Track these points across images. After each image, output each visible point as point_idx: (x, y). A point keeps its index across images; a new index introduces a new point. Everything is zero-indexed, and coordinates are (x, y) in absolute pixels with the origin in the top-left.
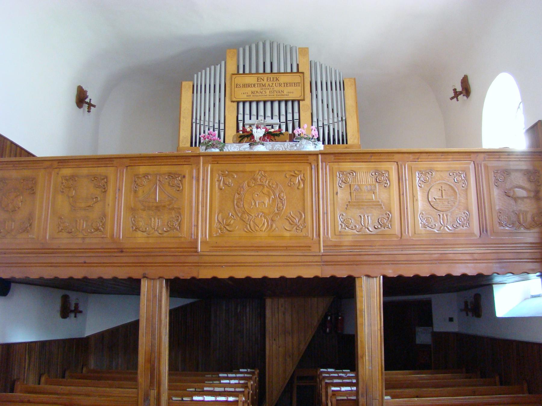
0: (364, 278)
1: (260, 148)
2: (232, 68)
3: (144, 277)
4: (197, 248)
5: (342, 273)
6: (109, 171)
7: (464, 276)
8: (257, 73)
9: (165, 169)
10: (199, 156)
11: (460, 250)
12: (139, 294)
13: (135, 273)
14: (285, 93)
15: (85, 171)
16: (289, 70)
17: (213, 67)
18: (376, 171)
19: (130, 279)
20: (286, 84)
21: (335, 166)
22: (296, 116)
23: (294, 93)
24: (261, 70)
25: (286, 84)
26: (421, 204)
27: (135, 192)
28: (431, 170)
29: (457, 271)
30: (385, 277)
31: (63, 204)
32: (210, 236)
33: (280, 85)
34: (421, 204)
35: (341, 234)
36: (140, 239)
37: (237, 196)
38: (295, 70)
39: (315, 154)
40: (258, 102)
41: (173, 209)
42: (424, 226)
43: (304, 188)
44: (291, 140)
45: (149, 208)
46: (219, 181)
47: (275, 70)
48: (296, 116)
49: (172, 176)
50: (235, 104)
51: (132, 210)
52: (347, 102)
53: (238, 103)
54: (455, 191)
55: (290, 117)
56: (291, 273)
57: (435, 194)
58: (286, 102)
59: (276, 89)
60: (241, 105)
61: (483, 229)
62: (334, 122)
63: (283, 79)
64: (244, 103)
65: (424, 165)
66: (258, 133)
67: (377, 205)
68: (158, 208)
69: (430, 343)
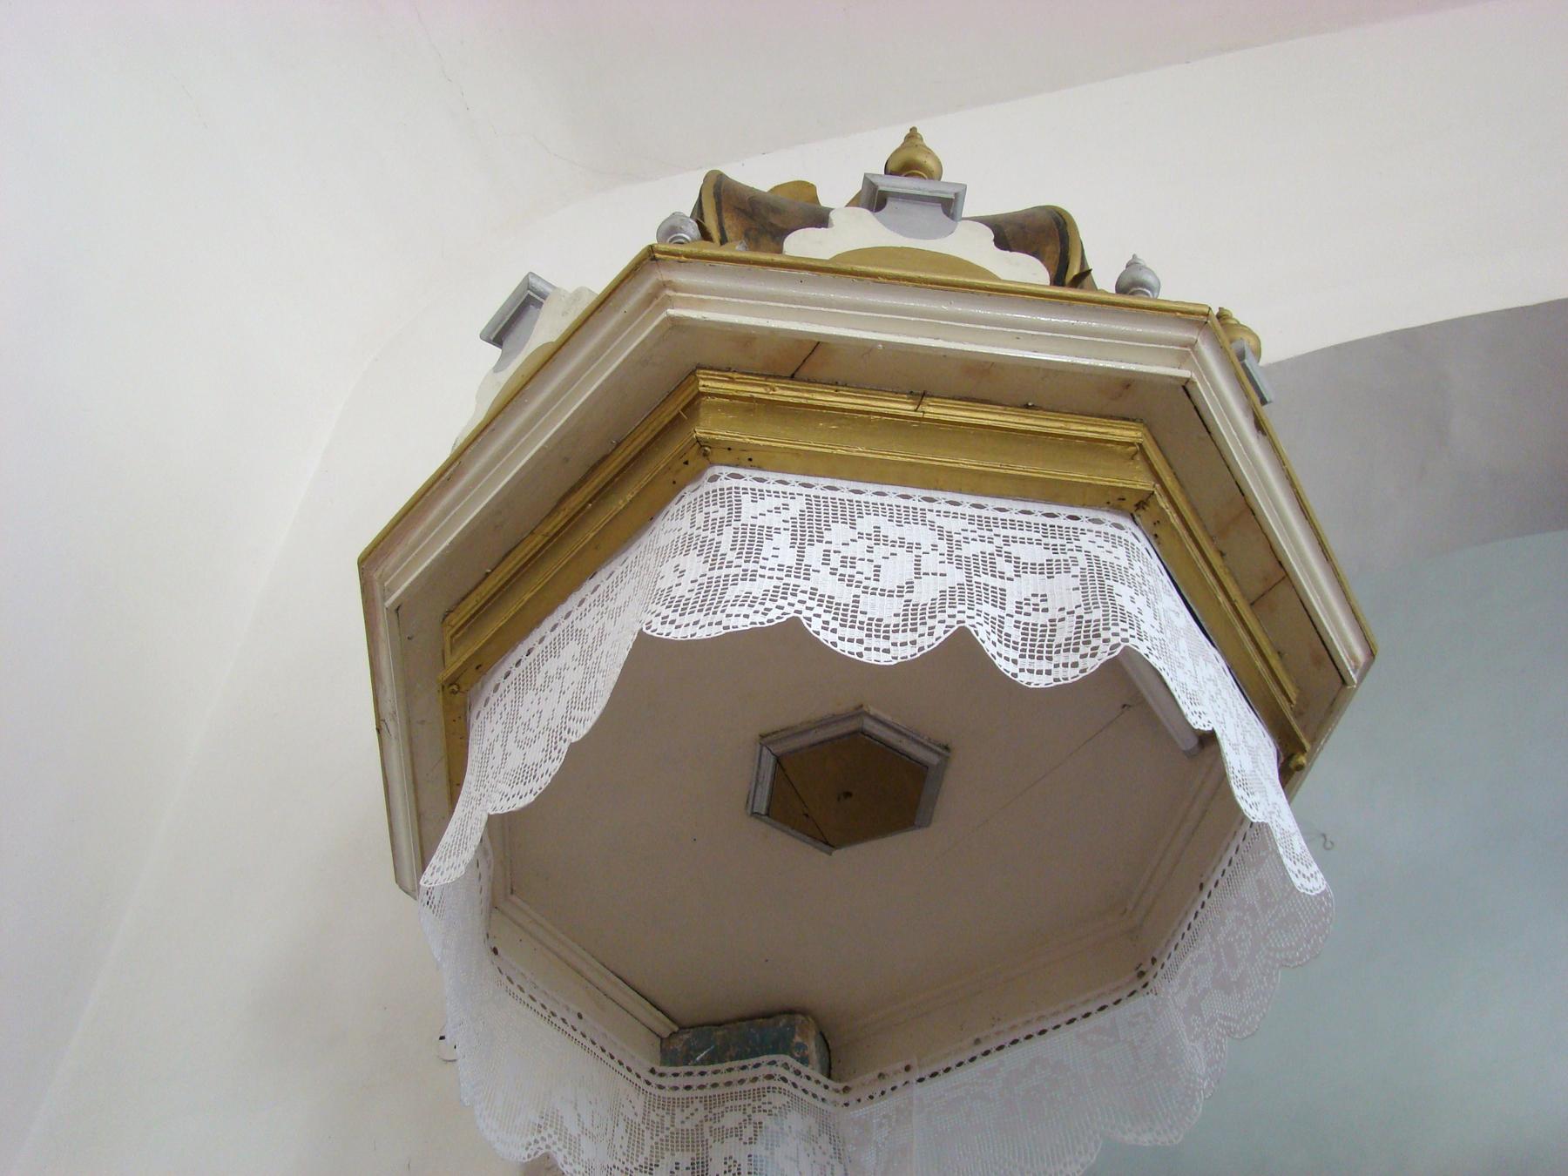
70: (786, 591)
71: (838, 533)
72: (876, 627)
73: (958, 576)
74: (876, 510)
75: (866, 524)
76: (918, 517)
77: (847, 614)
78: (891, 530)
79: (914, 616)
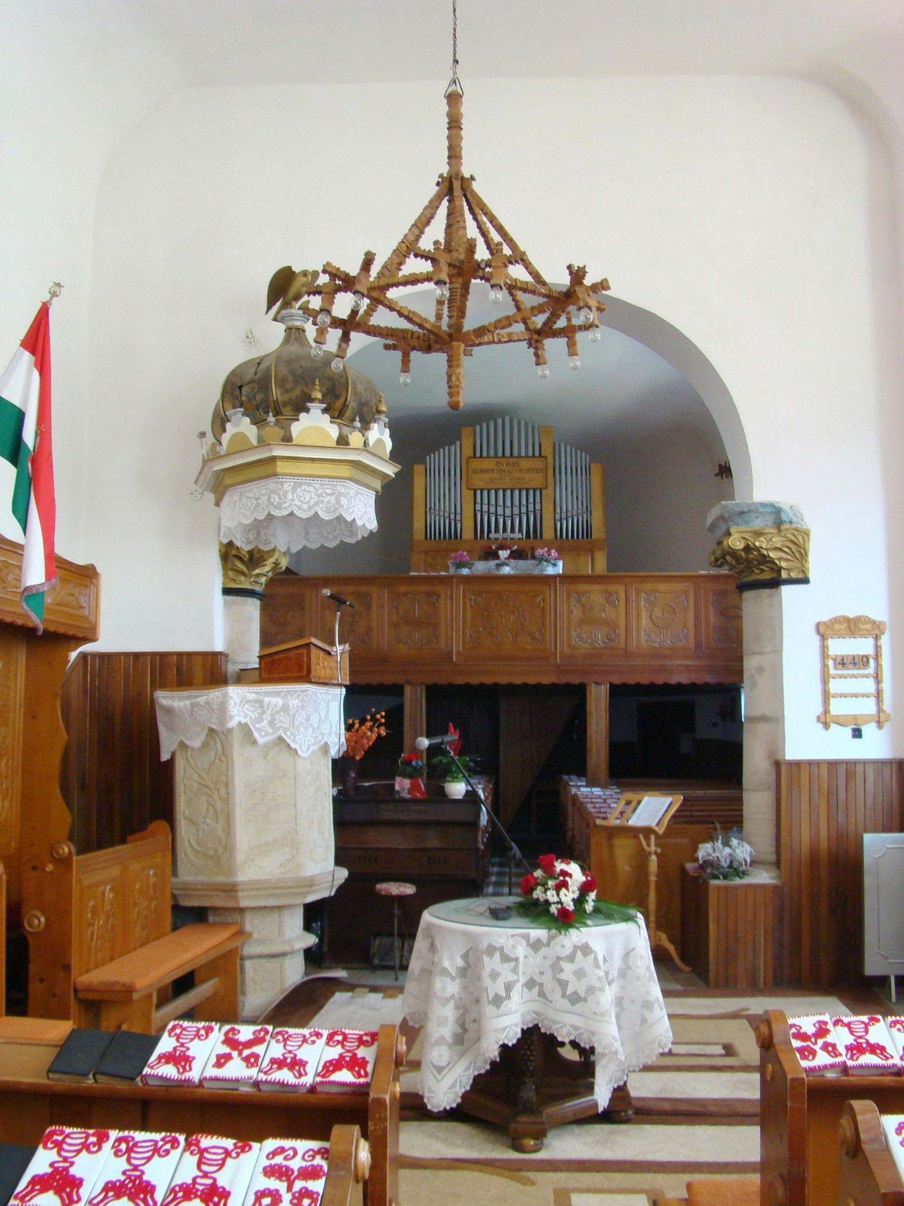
0: (593, 685)
1: (506, 570)
2: (468, 451)
3: (409, 683)
4: (451, 658)
5: (575, 680)
6: (374, 590)
7: (679, 685)
8: (496, 456)
9: (423, 588)
10: (452, 577)
11: (677, 662)
12: (403, 695)
13: (398, 679)
14: (527, 480)
16: (530, 454)
17: (447, 448)
18: (606, 592)
19: (395, 685)
20: (528, 471)
21: (572, 587)
22: (538, 507)
23: (536, 480)
24: (500, 454)
25: (528, 471)
26: (645, 621)
27: (397, 608)
28: (656, 591)
29: (674, 679)
30: (611, 685)
32: (463, 645)
33: (521, 471)
34: (645, 621)
35: (574, 648)
36: (402, 649)
37: (486, 613)
38: (537, 454)
39: (554, 577)
41: (430, 624)
42: (647, 641)
43: (543, 607)
44: (533, 557)
46: (471, 600)
47: (515, 453)
48: (538, 507)
49: (429, 594)
50: (472, 492)
51: (394, 625)
52: (593, 491)
53: (475, 491)
54: (674, 609)
55: (531, 508)
56: (532, 680)
57: (658, 613)
58: (527, 490)
59: (517, 475)
60: (479, 492)
61: (698, 645)
62: (578, 513)
64: (482, 491)
65: (649, 586)
66: (504, 554)
68: (417, 624)
70: (291, 505)
71: (299, 490)
72: (304, 511)
73: (317, 499)
74: (304, 484)
75: (303, 487)
76: (311, 485)
77: (299, 508)
78: (307, 489)
79: (310, 508)
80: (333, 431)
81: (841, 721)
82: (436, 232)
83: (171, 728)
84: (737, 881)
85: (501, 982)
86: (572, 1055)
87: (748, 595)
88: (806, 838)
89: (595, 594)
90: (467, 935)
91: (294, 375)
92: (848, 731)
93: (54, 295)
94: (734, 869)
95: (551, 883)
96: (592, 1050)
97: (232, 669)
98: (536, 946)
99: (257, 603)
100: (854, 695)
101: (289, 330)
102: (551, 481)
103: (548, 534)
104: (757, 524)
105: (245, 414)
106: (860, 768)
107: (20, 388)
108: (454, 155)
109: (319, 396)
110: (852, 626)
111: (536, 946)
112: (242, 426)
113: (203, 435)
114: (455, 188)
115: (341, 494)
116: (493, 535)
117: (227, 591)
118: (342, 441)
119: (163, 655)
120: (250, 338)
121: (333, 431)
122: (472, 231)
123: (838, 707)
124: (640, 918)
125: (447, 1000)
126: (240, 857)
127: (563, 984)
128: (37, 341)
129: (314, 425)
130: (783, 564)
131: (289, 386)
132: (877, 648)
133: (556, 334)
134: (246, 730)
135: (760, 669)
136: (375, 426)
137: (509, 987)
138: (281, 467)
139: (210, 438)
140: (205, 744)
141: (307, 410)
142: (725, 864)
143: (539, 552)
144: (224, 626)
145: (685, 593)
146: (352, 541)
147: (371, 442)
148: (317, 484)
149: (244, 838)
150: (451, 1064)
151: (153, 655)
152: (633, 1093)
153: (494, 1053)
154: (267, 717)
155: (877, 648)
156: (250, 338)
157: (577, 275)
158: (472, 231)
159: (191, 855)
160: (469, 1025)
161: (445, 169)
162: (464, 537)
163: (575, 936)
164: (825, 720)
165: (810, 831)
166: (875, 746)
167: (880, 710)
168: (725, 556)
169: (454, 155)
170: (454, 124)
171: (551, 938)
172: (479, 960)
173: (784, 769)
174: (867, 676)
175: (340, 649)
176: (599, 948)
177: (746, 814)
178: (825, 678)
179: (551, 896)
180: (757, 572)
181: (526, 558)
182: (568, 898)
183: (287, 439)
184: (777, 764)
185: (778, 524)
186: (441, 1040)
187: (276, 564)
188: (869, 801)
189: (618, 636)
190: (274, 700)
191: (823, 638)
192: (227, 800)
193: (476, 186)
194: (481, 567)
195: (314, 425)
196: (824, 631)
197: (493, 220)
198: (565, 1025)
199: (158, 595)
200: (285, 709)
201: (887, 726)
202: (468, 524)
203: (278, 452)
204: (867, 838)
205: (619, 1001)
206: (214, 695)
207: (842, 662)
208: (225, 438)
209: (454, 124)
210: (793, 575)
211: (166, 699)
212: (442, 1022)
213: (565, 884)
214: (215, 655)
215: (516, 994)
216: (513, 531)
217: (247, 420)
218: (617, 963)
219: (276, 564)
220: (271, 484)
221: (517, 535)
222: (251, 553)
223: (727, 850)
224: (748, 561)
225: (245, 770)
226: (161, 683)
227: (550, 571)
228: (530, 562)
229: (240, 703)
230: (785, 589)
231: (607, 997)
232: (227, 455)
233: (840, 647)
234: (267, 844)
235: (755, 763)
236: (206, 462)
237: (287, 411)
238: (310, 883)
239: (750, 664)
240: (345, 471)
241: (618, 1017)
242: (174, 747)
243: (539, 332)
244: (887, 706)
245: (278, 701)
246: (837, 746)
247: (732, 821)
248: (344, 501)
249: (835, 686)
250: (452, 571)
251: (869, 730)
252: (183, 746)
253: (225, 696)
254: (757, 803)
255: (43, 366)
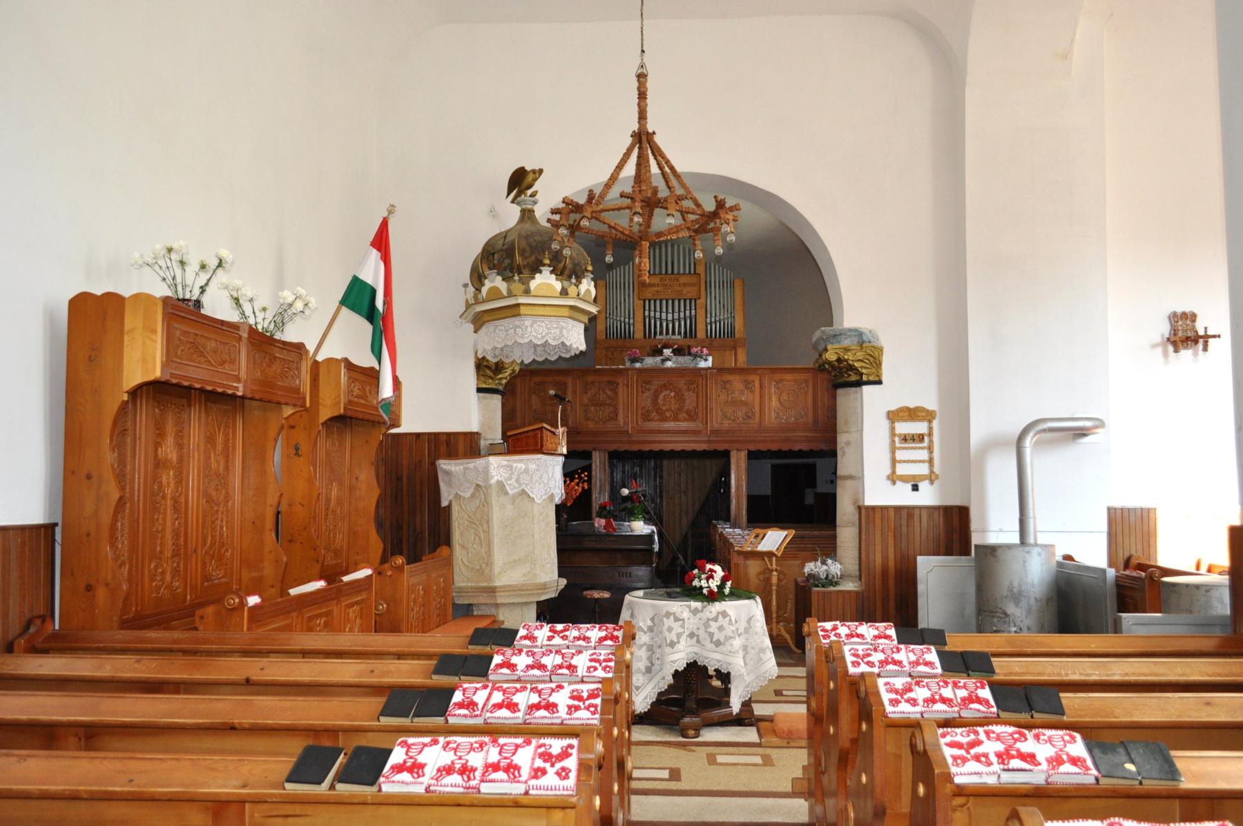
1: (669, 364)
5: (721, 447)
7: (801, 451)
9: (606, 379)
13: (587, 447)
15: (550, 379)
19: (585, 451)
20: (685, 285)
23: (690, 292)
25: (685, 285)
28: (782, 380)
29: (797, 447)
31: (535, 400)
34: (775, 403)
40: (661, 301)
44: (690, 354)
45: (596, 405)
49: (610, 383)
57: (785, 397)
61: (816, 420)
63: (683, 280)
65: (777, 376)
66: (667, 352)
67: (745, 404)
69: (769, 492)
80: (558, 286)
81: (904, 479)
82: (630, 170)
83: (449, 484)
84: (832, 588)
85: (674, 632)
86: (716, 683)
87: (840, 392)
88: (879, 560)
89: (737, 382)
90: (653, 606)
91: (531, 246)
92: (909, 486)
93: (390, 212)
94: (830, 581)
95: (703, 576)
96: (729, 674)
97: (483, 444)
98: (695, 612)
99: (500, 397)
100: (914, 461)
101: (523, 211)
102: (703, 293)
103: (701, 334)
104: (846, 343)
105: (498, 274)
106: (917, 512)
107: (372, 272)
108: (642, 116)
109: (547, 261)
110: (912, 414)
111: (695, 612)
112: (495, 282)
113: (466, 286)
114: (643, 139)
115: (563, 328)
116: (658, 337)
117: (479, 390)
118: (564, 293)
119: (436, 435)
120: (493, 213)
121: (558, 286)
122: (654, 169)
123: (901, 470)
124: (758, 599)
125: (641, 646)
126: (497, 570)
127: (711, 635)
128: (381, 242)
129: (545, 280)
130: (864, 371)
131: (527, 254)
132: (931, 429)
133: (706, 231)
134: (501, 485)
135: (848, 443)
136: (584, 281)
137: (679, 635)
138: (523, 310)
139: (471, 289)
140: (473, 495)
141: (540, 272)
142: (823, 576)
143: (694, 350)
144: (474, 413)
145: (806, 381)
146: (568, 356)
147: (582, 292)
148: (547, 320)
149: (499, 557)
150: (644, 685)
151: (429, 434)
152: (756, 713)
153: (670, 680)
154: (515, 477)
155: (931, 429)
156: (493, 213)
157: (720, 204)
158: (654, 169)
159: (463, 570)
160: (657, 662)
161: (636, 127)
162: (637, 336)
163: (718, 607)
164: (893, 478)
165: (883, 554)
166: (927, 497)
167: (932, 472)
168: (822, 368)
169: (642, 116)
170: (642, 95)
171: (704, 607)
172: (662, 621)
173: (863, 511)
174: (922, 448)
175: (561, 430)
176: (730, 612)
177: (838, 543)
178: (893, 450)
179: (704, 583)
180: (846, 374)
181: (684, 355)
182: (714, 584)
183: (527, 292)
184: (860, 508)
185: (861, 344)
186: (639, 670)
187: (513, 371)
188: (924, 533)
189: (754, 414)
190: (519, 465)
191: (893, 422)
192: (488, 532)
193: (657, 139)
194: (650, 362)
195: (545, 280)
196: (894, 416)
197: (668, 162)
198: (713, 659)
199: (436, 393)
200: (527, 471)
201: (936, 483)
202: (639, 326)
203: (522, 300)
204: (920, 559)
205: (745, 648)
206: (479, 462)
207: (905, 439)
208: (484, 290)
209: (642, 95)
210: (871, 378)
211: (444, 465)
212: (640, 659)
213: (712, 577)
214: (471, 433)
215: (683, 641)
216: (674, 333)
217: (499, 278)
218: (742, 625)
219: (513, 371)
220: (516, 321)
221: (677, 337)
222: (497, 364)
223: (825, 567)
224: (841, 369)
225: (499, 513)
226: (452, 454)
227: (702, 364)
228: (687, 358)
229: (498, 467)
230: (865, 388)
231: (737, 643)
232: (484, 301)
233: (904, 428)
234: (515, 561)
235: (845, 509)
236: (468, 306)
237: (526, 274)
238: (544, 587)
239: (842, 439)
240: (566, 312)
241: (744, 658)
242: (451, 497)
243: (696, 231)
244: (936, 469)
245: (521, 466)
246: (901, 496)
247: (829, 549)
248: (565, 332)
249: (900, 455)
250: (628, 364)
251: (924, 486)
252: (457, 496)
253: (488, 464)
254: (847, 535)
255: (386, 259)
